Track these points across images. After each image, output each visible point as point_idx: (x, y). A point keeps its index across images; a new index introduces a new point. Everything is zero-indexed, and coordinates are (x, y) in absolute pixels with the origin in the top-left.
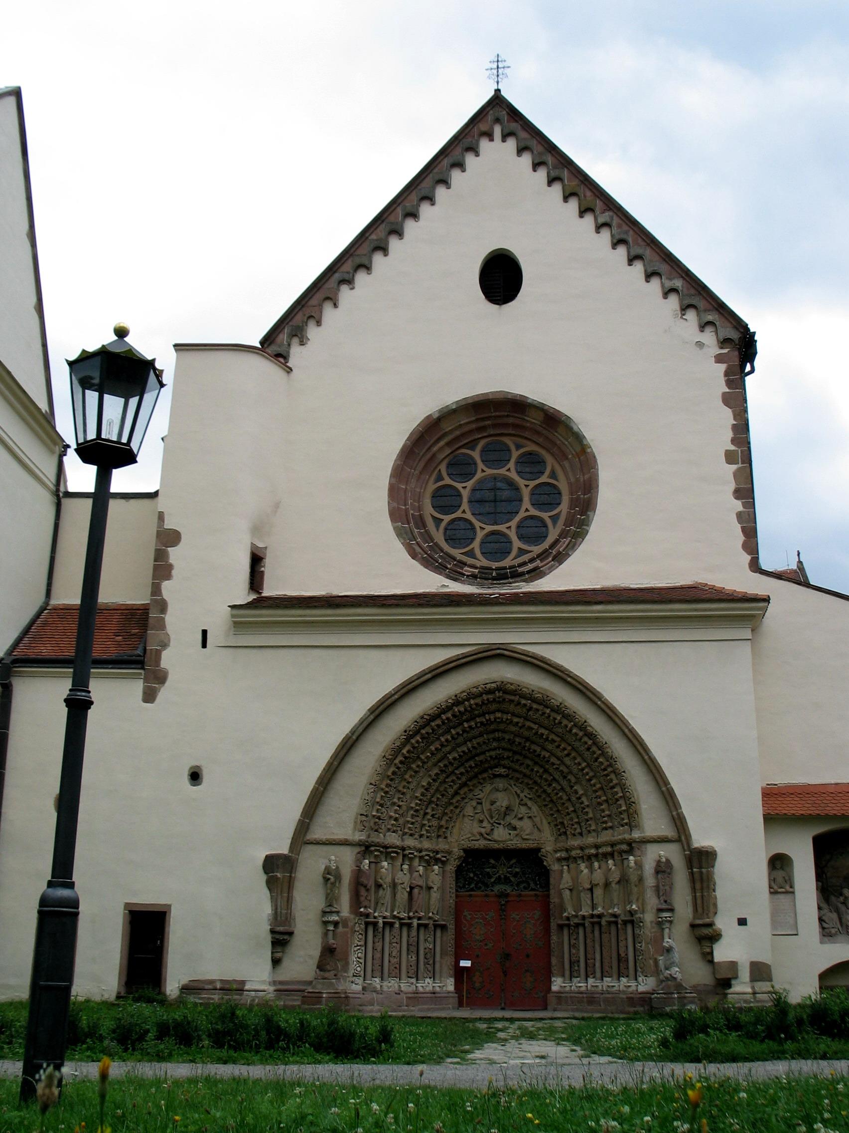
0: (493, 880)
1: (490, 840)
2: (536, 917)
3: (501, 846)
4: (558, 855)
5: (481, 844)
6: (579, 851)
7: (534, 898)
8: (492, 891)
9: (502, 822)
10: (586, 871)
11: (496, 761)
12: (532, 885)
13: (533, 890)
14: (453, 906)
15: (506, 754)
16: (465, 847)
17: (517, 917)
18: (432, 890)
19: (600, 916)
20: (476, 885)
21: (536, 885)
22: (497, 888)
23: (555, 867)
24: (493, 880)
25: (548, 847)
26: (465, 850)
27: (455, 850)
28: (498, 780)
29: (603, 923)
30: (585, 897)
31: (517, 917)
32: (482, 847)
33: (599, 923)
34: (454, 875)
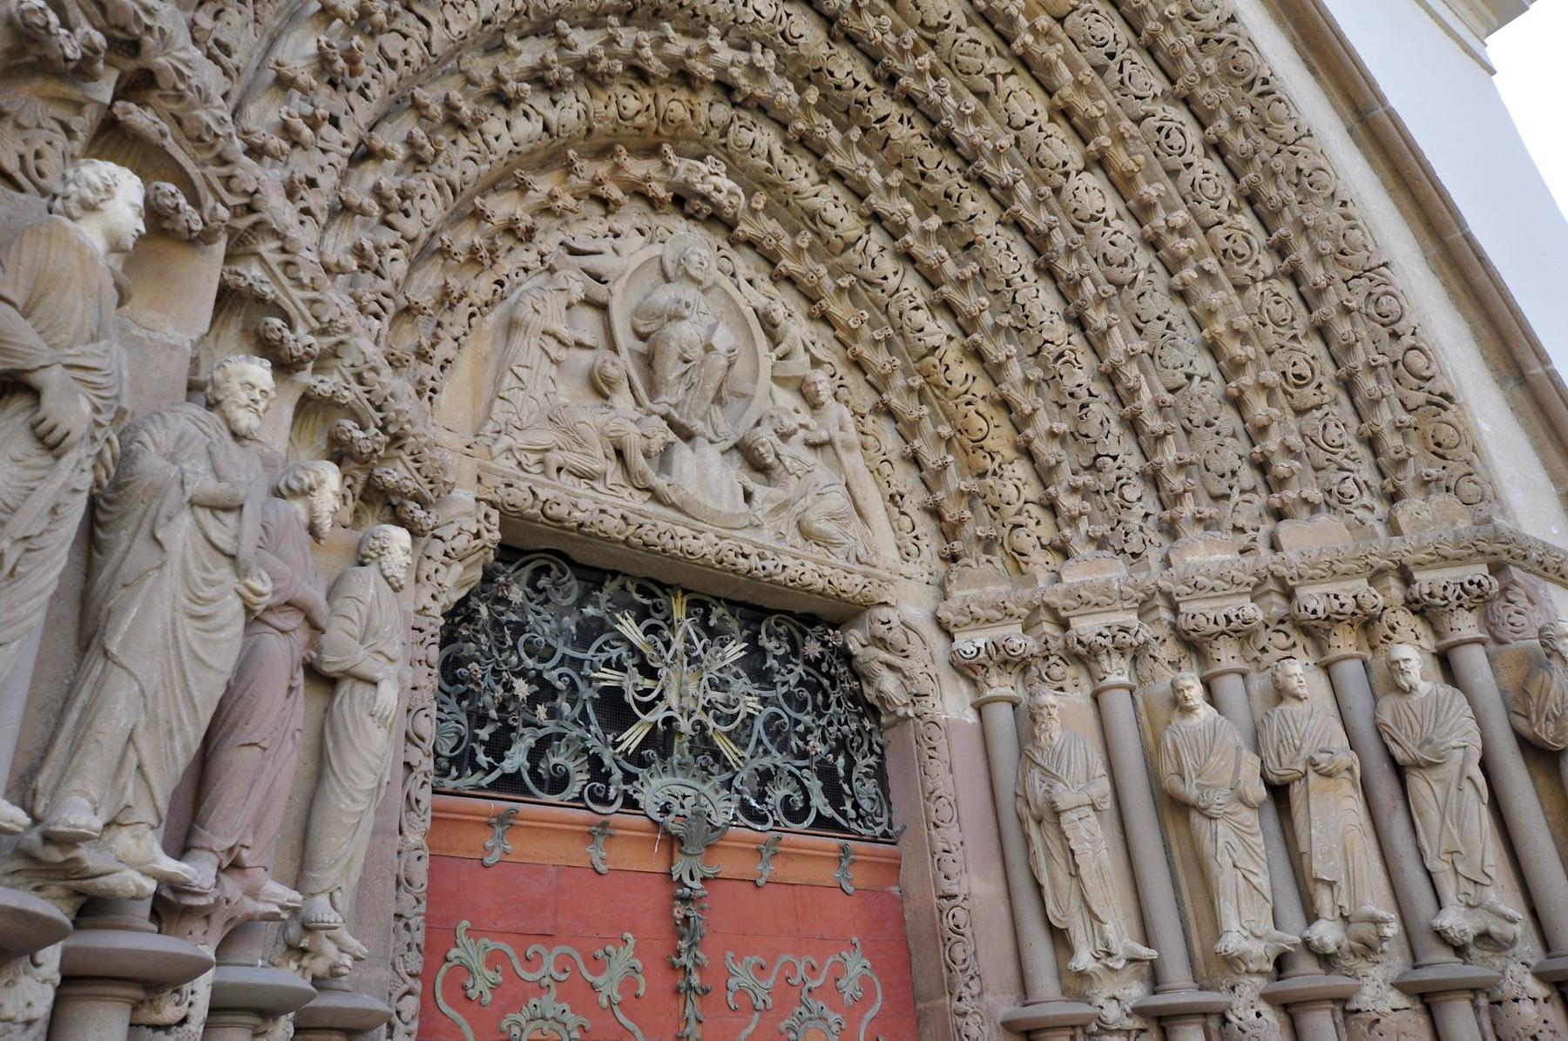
0: (633, 737)
1: (656, 496)
2: (849, 987)
3: (704, 545)
4: (971, 642)
5: (604, 506)
6: (1131, 619)
7: (830, 874)
8: (631, 803)
9: (697, 425)
10: (1204, 712)
11: (722, 112)
12: (819, 802)
13: (822, 822)
14: (420, 872)
15: (784, 93)
16: (519, 496)
17: (762, 990)
18: (350, 698)
19: (1326, 960)
20: (535, 754)
21: (834, 795)
22: (654, 789)
23: (952, 704)
24: (633, 737)
25: (910, 604)
26: (510, 518)
27: (464, 496)
28: (679, 225)
29: (1376, 990)
30: (1240, 848)
31: (762, 990)
32: (612, 525)
33: (1342, 1004)
34: (434, 654)
